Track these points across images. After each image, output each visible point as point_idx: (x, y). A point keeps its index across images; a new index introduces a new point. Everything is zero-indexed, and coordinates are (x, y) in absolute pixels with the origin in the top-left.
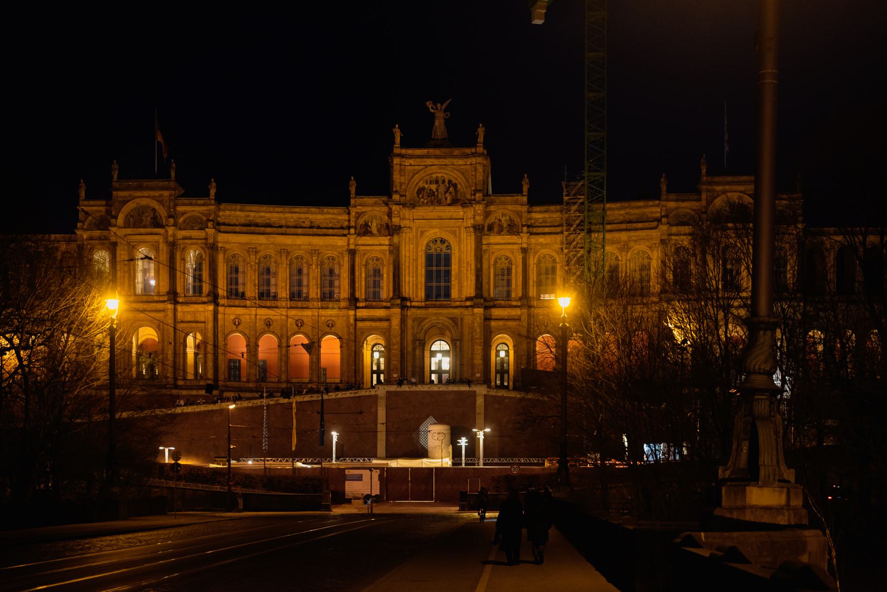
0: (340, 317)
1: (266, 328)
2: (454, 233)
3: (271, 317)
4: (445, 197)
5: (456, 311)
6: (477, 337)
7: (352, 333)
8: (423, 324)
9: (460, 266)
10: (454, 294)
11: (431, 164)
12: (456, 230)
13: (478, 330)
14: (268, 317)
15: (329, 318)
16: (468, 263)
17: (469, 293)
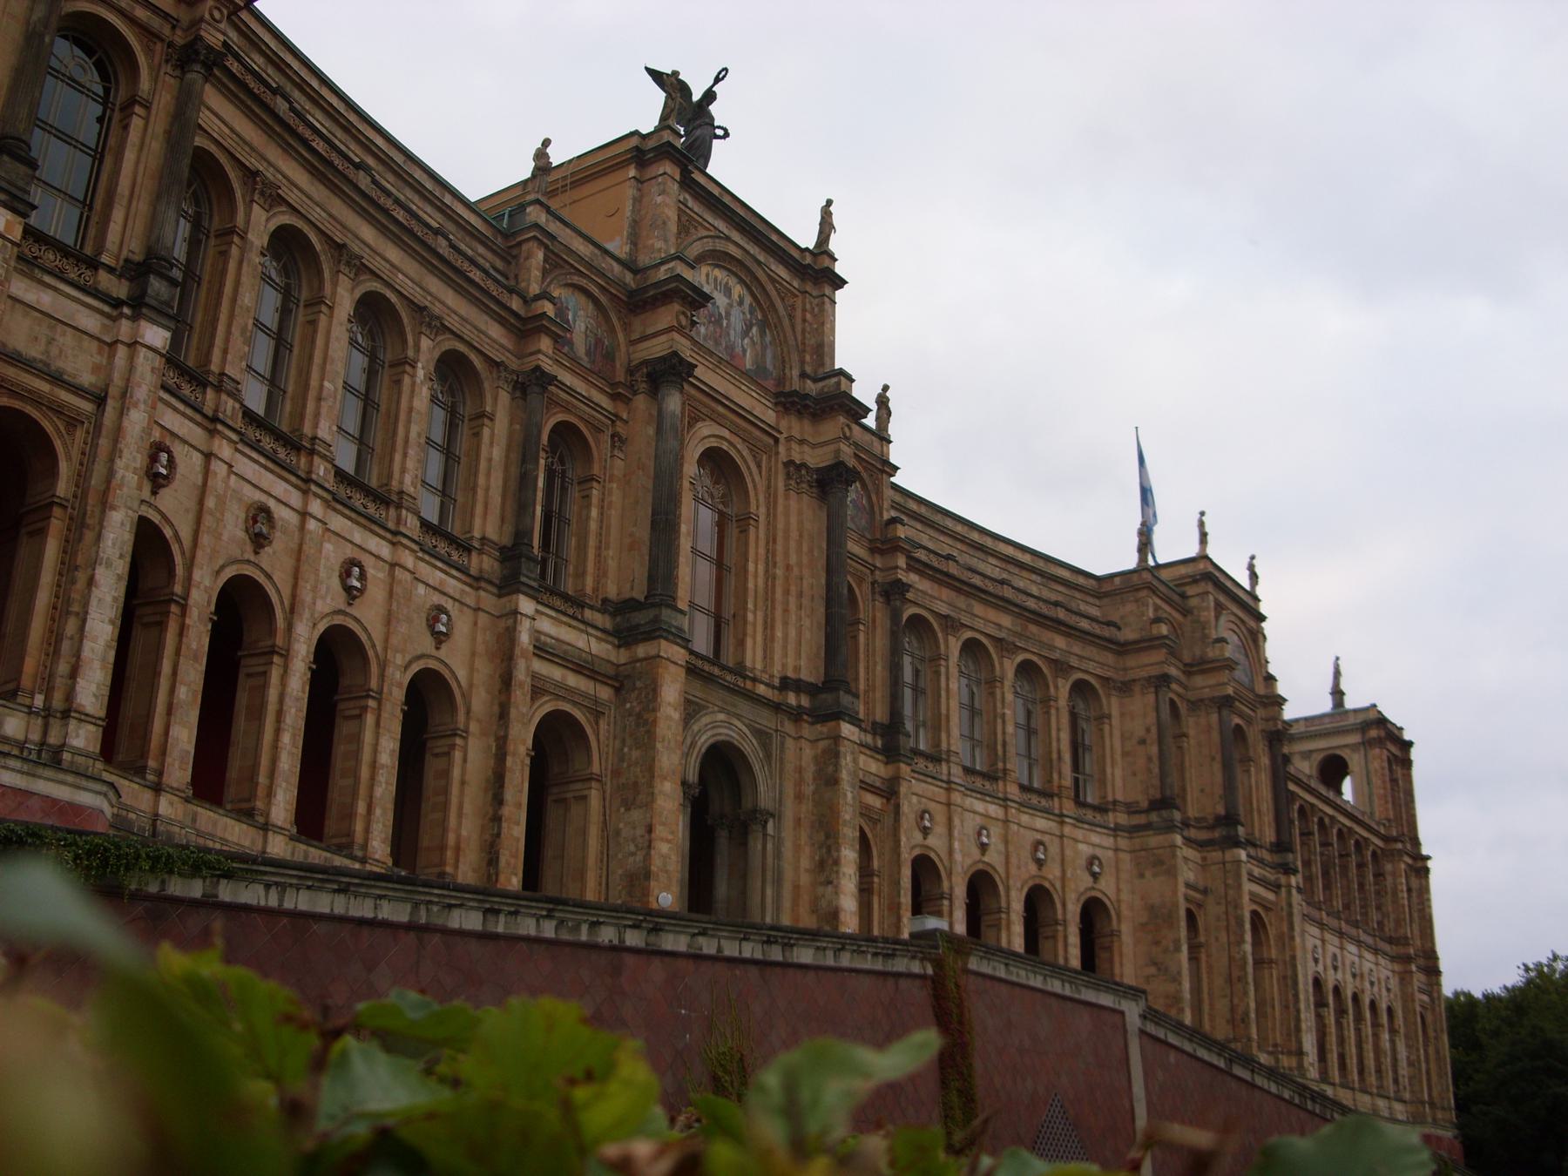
0: (465, 608)
1: (249, 548)
2: (759, 466)
3: (272, 503)
4: (742, 346)
5: (766, 719)
6: (847, 817)
7: (521, 685)
8: (696, 728)
9: (770, 577)
10: (753, 657)
11: (726, 231)
12: (761, 460)
13: (849, 795)
14: (263, 498)
15: (437, 599)
16: (788, 568)
17: (791, 661)
